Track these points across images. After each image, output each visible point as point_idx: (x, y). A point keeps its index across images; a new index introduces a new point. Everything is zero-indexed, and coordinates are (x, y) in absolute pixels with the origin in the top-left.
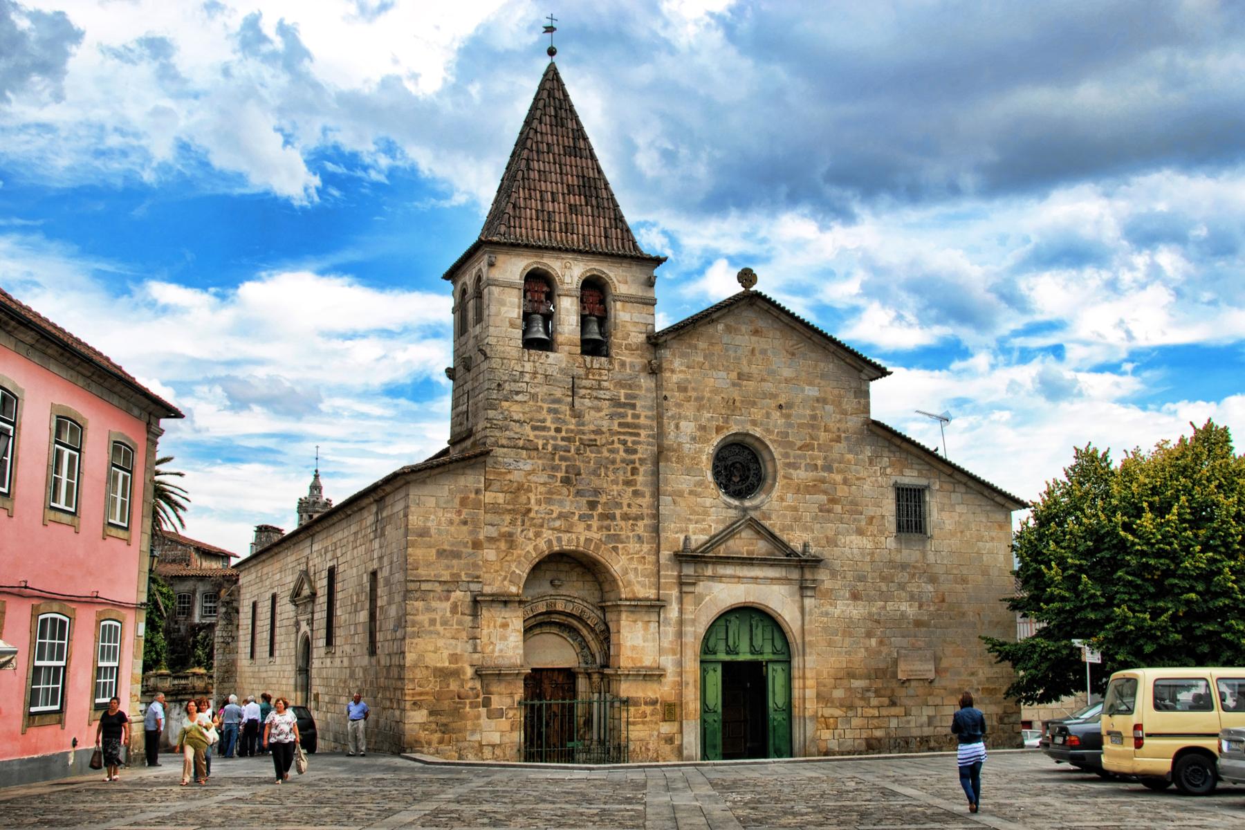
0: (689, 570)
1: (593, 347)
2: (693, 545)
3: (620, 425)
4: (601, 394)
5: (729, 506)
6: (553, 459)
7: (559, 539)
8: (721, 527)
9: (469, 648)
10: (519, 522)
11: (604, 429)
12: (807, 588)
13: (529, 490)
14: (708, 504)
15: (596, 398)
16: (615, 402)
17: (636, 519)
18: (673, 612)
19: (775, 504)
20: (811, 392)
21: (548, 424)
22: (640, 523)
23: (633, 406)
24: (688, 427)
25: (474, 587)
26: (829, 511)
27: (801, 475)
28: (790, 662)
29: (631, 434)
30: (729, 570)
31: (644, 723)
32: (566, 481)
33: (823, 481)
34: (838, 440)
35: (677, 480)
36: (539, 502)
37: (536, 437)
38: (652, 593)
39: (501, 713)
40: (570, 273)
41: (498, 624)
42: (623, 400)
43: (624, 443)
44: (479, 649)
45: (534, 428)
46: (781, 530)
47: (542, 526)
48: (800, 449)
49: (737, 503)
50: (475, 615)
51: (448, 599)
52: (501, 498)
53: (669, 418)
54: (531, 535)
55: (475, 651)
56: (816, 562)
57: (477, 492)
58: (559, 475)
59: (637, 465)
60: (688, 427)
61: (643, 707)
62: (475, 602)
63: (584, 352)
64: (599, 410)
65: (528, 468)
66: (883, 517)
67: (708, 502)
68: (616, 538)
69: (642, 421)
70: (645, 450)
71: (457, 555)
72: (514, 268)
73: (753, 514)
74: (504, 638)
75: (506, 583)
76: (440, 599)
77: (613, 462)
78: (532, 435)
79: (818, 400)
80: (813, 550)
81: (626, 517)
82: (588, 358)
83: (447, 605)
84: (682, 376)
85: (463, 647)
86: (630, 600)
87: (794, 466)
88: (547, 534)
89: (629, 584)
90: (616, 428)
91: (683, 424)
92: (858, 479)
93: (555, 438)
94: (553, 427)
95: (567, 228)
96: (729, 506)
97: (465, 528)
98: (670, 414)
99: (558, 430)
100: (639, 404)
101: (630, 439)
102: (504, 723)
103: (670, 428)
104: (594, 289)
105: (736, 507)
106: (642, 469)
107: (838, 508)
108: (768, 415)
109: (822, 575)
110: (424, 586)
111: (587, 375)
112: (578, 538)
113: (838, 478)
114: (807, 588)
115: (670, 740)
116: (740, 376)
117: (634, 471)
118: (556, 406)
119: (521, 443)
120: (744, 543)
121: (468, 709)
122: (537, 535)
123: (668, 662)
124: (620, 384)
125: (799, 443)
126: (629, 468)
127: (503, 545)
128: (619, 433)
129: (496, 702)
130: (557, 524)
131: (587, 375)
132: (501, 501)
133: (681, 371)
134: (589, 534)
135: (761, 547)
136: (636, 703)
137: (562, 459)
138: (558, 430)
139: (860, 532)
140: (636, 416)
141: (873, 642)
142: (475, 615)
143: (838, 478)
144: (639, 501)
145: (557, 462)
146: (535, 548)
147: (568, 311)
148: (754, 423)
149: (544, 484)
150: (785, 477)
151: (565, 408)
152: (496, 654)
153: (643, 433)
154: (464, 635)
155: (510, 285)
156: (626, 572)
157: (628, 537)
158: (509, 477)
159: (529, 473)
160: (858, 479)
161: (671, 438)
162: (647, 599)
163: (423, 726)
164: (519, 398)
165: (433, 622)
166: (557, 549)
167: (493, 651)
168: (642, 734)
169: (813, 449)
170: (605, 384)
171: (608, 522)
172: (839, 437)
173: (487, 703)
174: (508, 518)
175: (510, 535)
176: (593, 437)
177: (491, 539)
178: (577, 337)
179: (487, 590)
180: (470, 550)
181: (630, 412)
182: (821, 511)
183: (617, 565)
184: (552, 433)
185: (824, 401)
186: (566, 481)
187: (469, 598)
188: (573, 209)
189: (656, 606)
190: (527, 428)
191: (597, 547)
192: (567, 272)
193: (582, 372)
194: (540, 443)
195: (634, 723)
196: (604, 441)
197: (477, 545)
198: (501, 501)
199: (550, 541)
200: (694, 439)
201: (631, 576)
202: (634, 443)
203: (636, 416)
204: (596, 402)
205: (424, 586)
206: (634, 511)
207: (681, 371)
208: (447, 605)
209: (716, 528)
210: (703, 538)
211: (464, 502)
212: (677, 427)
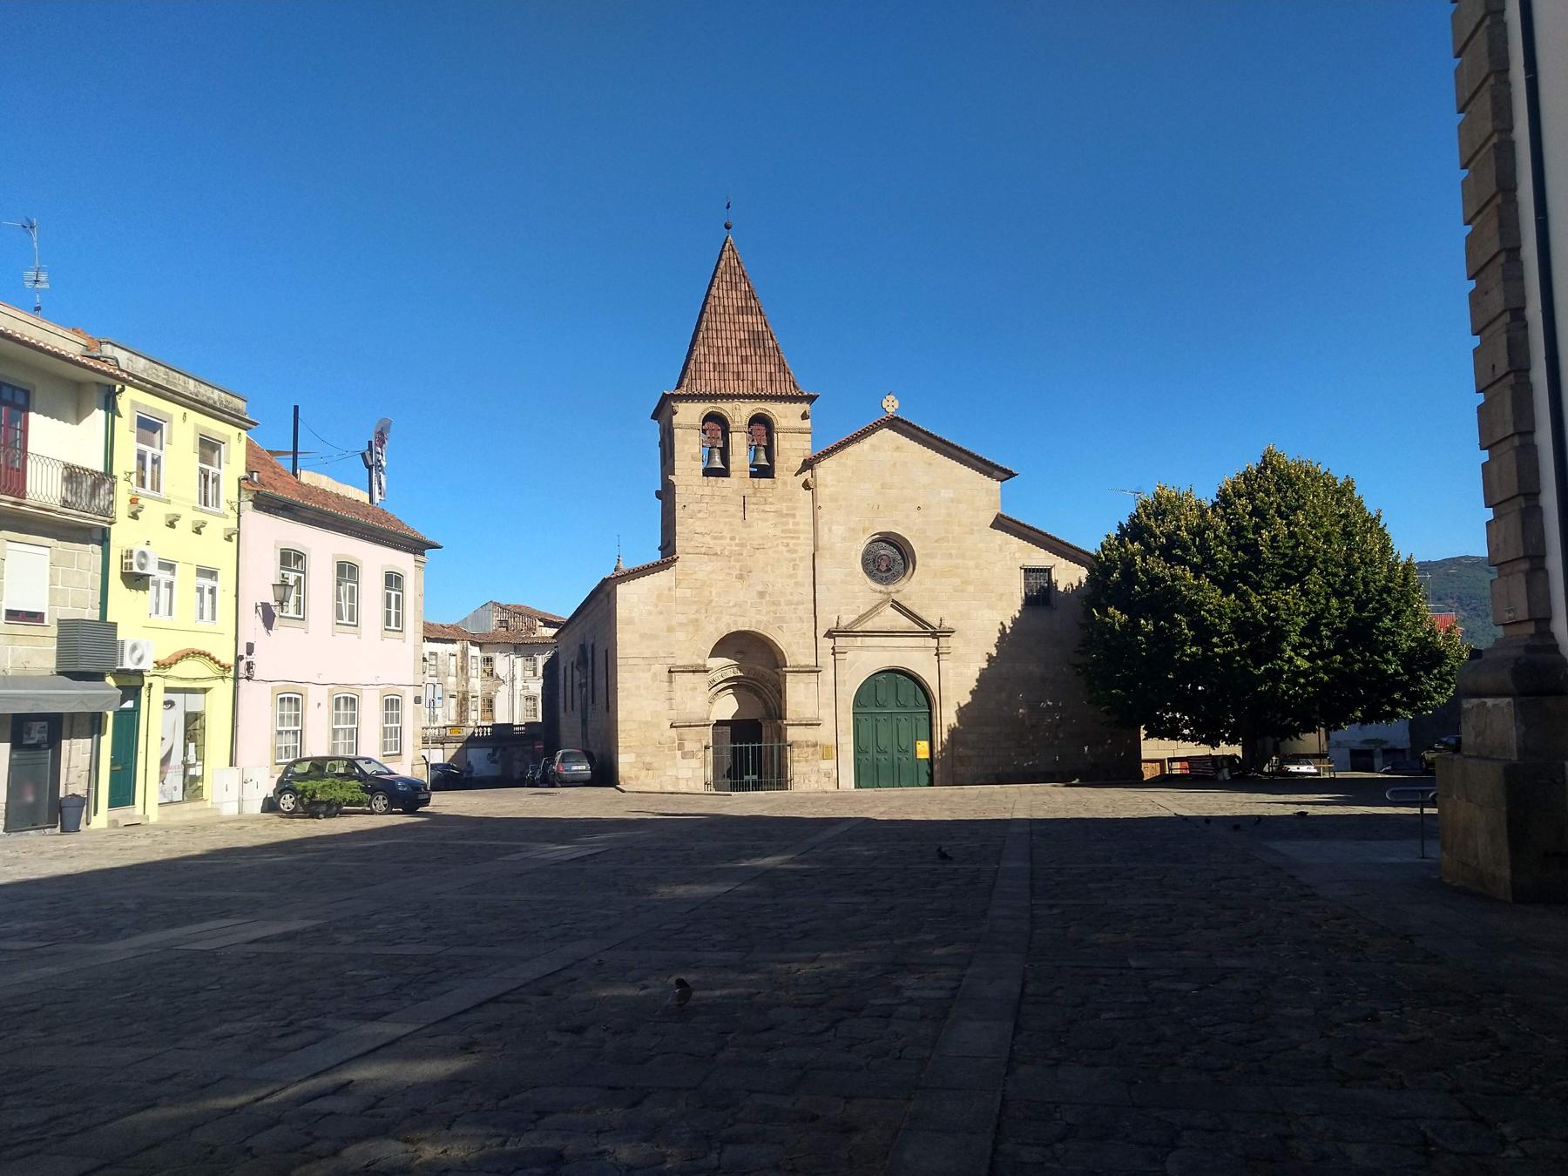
0: (840, 641)
2: (843, 624)
4: (767, 508)
7: (735, 623)
13: (711, 586)
18: (828, 674)
19: (911, 589)
20: (947, 494)
23: (794, 516)
24: (839, 530)
25: (670, 661)
28: (930, 714)
30: (868, 641)
32: (740, 577)
39: (692, 755)
40: (739, 413)
45: (715, 538)
49: (882, 588)
50: (671, 682)
52: (688, 593)
56: (949, 632)
58: (735, 572)
63: (753, 475)
64: (766, 520)
65: (709, 569)
67: (857, 588)
68: (782, 619)
69: (801, 527)
73: (895, 597)
80: (947, 624)
81: (789, 603)
83: (648, 675)
90: (778, 532)
91: (834, 528)
99: (733, 538)
101: (791, 542)
102: (695, 763)
104: (762, 422)
106: (802, 565)
107: (971, 589)
109: (952, 642)
110: (631, 662)
113: (971, 563)
115: (828, 775)
120: (890, 618)
122: (718, 619)
123: (827, 715)
129: (688, 746)
130: (734, 610)
135: (904, 623)
137: (737, 561)
138: (733, 538)
139: (991, 607)
140: (797, 524)
141: (1004, 695)
142: (671, 682)
143: (971, 563)
147: (740, 444)
148: (896, 523)
151: (738, 521)
155: (692, 427)
156: (790, 645)
161: (824, 538)
163: (632, 765)
165: (638, 687)
174: (695, 608)
177: (681, 624)
179: (680, 663)
181: (791, 521)
183: (782, 640)
185: (959, 501)
186: (740, 577)
188: (745, 360)
189: (815, 671)
190: (708, 539)
191: (766, 627)
193: (751, 491)
197: (670, 629)
200: (844, 539)
201: (794, 648)
203: (797, 524)
205: (631, 662)
206: (796, 598)
208: (648, 675)
211: (659, 597)
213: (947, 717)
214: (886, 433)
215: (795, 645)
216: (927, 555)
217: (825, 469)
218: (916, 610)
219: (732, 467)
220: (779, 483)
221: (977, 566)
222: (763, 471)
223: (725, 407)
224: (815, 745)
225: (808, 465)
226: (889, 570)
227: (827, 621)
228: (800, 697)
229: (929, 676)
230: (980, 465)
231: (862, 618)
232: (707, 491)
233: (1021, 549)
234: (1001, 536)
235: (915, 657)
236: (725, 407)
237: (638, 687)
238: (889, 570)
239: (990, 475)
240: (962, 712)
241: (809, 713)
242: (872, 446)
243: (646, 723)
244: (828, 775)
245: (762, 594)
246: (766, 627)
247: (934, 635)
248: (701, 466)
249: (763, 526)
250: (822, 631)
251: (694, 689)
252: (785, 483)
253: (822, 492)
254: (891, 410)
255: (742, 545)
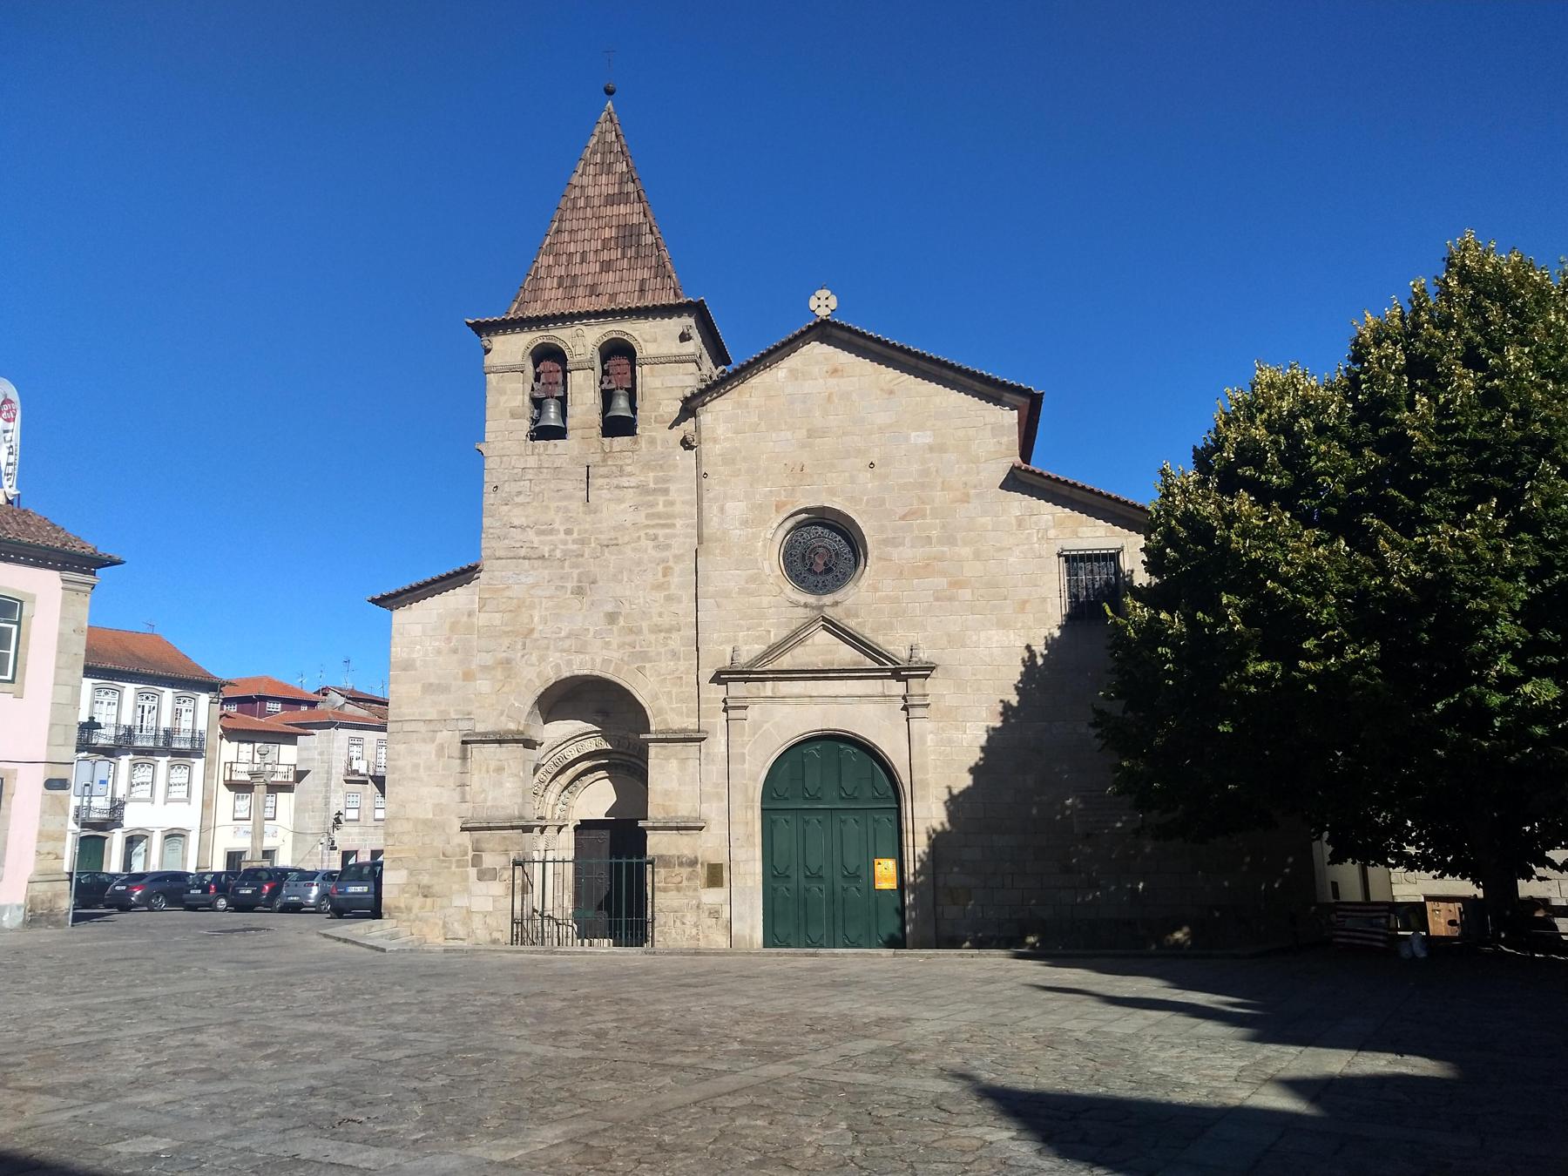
0: (737, 689)
1: (617, 426)
2: (744, 659)
3: (648, 516)
4: (624, 481)
5: (796, 604)
6: (562, 568)
7: (569, 663)
8: (785, 633)
9: (457, 796)
10: (519, 646)
11: (628, 524)
12: (913, 706)
13: (532, 606)
14: (765, 604)
15: (617, 487)
16: (642, 489)
17: (669, 631)
18: (717, 744)
21: (556, 526)
22: (674, 635)
23: (666, 491)
24: (736, 508)
25: (465, 725)
26: (951, 599)
27: (906, 554)
28: (899, 810)
29: (663, 526)
31: (678, 890)
32: (579, 591)
33: (941, 558)
34: (966, 499)
35: (721, 575)
36: (544, 621)
37: (542, 543)
38: (690, 723)
40: (583, 341)
41: (492, 768)
42: (652, 485)
43: (655, 538)
44: (468, 797)
45: (541, 533)
46: (873, 630)
47: (548, 648)
48: (903, 518)
49: (811, 599)
50: (464, 758)
51: (433, 741)
52: (497, 619)
53: (710, 500)
54: (534, 659)
55: (464, 801)
56: (926, 670)
57: (470, 615)
58: (569, 585)
59: (671, 564)
60: (736, 508)
61: (677, 870)
62: (464, 742)
64: (620, 501)
65: (530, 580)
66: (1044, 600)
68: (644, 656)
69: (678, 508)
70: (683, 539)
71: (443, 689)
72: (511, 348)
73: (830, 613)
74: (500, 784)
75: (503, 718)
76: (424, 741)
77: (639, 563)
78: (536, 540)
79: (931, 449)
80: (924, 655)
81: (656, 629)
82: (607, 440)
84: (727, 445)
85: (449, 796)
86: (662, 732)
87: (893, 542)
88: (554, 657)
89: (660, 711)
90: (641, 518)
91: (729, 505)
92: (1001, 549)
93: (565, 543)
94: (562, 529)
95: (593, 290)
96: (796, 604)
97: (455, 657)
98: (711, 495)
99: (568, 532)
100: (673, 487)
101: (661, 532)
103: (711, 511)
105: (806, 605)
106: (677, 569)
107: (966, 594)
108: (853, 480)
109: (933, 687)
111: (604, 460)
112: (593, 660)
114: (913, 706)
115: (714, 914)
116: (811, 434)
117: (667, 572)
118: (565, 503)
119: (523, 552)
120: (823, 648)
121: (454, 868)
122: (542, 659)
124: (647, 466)
125: (901, 511)
126: (660, 568)
127: (499, 674)
128: (647, 526)
129: (489, 860)
131: (604, 460)
132: (498, 622)
133: (727, 439)
134: (607, 654)
135: (846, 655)
136: (666, 862)
138: (568, 532)
139: (1003, 625)
140: (672, 503)
142: (464, 758)
143: (966, 551)
144: (674, 607)
145: (567, 570)
146: (539, 675)
147: (584, 392)
148: (832, 492)
149: (551, 597)
150: (880, 559)
151: (576, 506)
152: (489, 804)
153: (679, 523)
154: (451, 783)
156: (655, 697)
157: (659, 654)
158: (507, 593)
159: (533, 586)
160: (1001, 549)
161: (713, 525)
162: (684, 731)
163: (403, 889)
164: (518, 500)
165: (416, 767)
166: (566, 674)
167: (485, 800)
168: (675, 904)
169: (924, 516)
170: (628, 469)
171: (629, 639)
172: (968, 495)
173: (476, 861)
174: (506, 641)
175: (508, 661)
176: (613, 535)
178: (596, 419)
179: (480, 728)
180: (460, 683)
181: (661, 499)
182: (937, 599)
184: (562, 536)
185: (941, 449)
186: (579, 591)
187: (458, 740)
188: (606, 266)
189: (694, 738)
190: (531, 534)
191: (618, 670)
192: (579, 341)
194: (546, 551)
195: (665, 890)
196: (626, 539)
197: (468, 676)
198: (498, 622)
199: (558, 666)
200: (745, 523)
201: (663, 702)
202: (666, 537)
203: (672, 503)
204: (617, 492)
205: (407, 727)
206: (666, 621)
207: (727, 439)
208: (431, 748)
209: (774, 638)
210: (759, 648)
211: (454, 627)
212: (722, 510)
213: (927, 814)
214: (816, 352)
215: (664, 698)
216: (886, 542)
217: (716, 413)
218: (867, 633)
219: (570, 422)
220: (643, 444)
221: (977, 556)
222: (617, 426)
223: (562, 335)
224: (693, 863)
225: (690, 407)
226: (828, 570)
227: (718, 654)
228: (671, 781)
229: (891, 745)
230: (978, 386)
231: (775, 650)
232: (532, 462)
233: (1059, 524)
234: (1019, 503)
235: (866, 713)
236: (562, 335)
237: (416, 767)
238: (828, 570)
239: (998, 401)
240: (955, 803)
241: (684, 809)
242: (793, 374)
243: (425, 822)
244: (714, 914)
245: (612, 618)
246: (618, 670)
247: (897, 674)
248: (526, 425)
249: (616, 509)
250: (708, 673)
251: (500, 770)
252: (652, 441)
253: (711, 450)
254: (823, 313)
255: (582, 542)
